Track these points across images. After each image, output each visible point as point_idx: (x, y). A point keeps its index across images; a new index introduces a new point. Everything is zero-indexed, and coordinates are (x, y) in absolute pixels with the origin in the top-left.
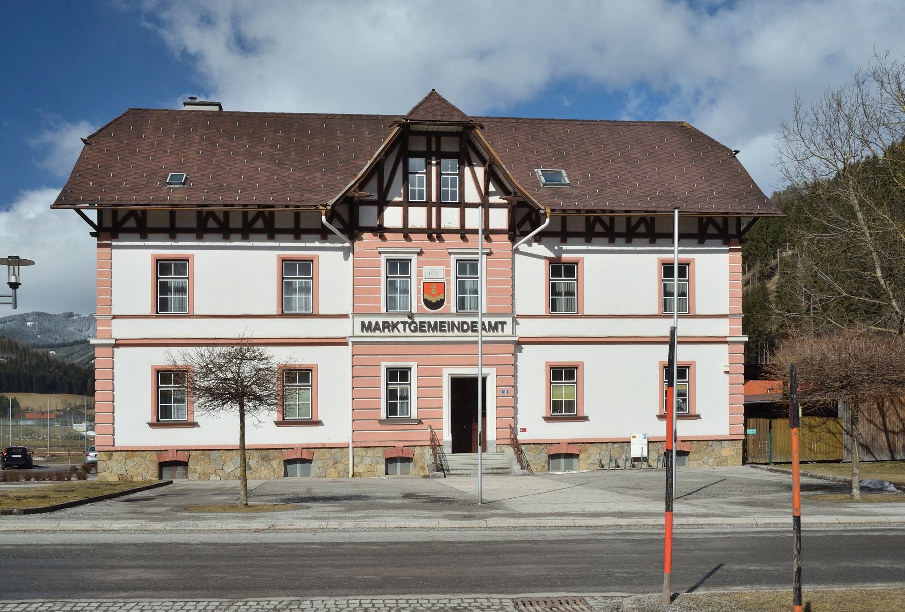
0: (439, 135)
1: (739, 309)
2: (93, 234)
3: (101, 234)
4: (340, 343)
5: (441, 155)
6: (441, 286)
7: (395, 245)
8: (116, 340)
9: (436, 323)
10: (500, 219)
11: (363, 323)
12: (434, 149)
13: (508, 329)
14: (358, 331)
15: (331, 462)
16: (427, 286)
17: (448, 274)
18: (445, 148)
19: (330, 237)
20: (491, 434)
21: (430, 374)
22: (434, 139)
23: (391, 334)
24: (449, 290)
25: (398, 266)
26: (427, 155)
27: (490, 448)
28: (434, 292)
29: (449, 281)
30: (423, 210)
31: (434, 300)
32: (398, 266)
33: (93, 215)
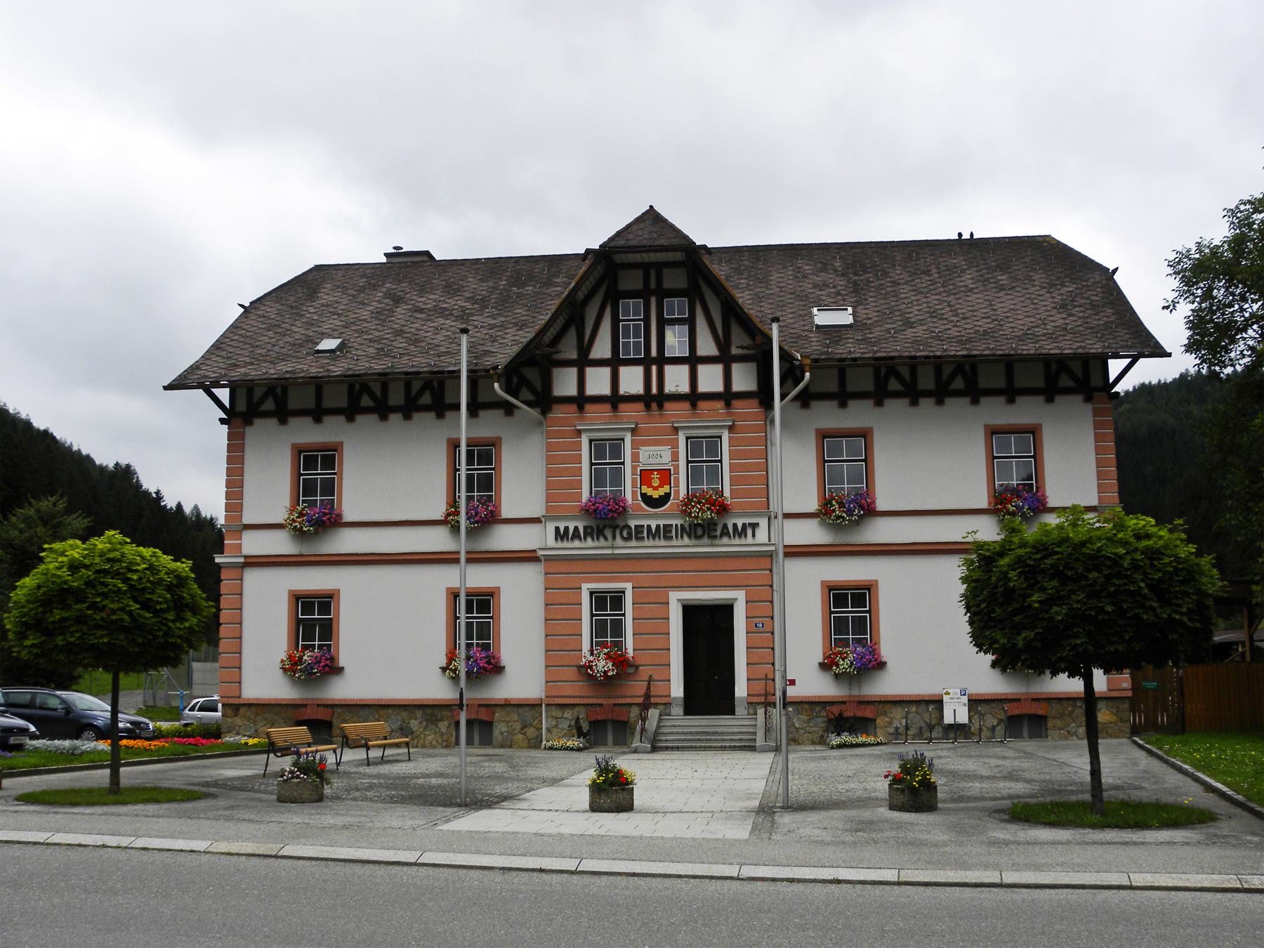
0: (659, 267)
1: (1114, 496)
2: (222, 421)
3: (234, 421)
4: (527, 557)
5: (664, 294)
6: (666, 476)
7: (598, 422)
8: (246, 557)
9: (658, 526)
10: (744, 379)
11: (557, 529)
12: (653, 285)
13: (762, 535)
14: (551, 541)
15: (518, 726)
16: (645, 476)
17: (675, 457)
18: (668, 284)
19: (515, 411)
20: (741, 689)
21: (653, 601)
22: (653, 273)
23: (596, 544)
24: (677, 480)
25: (606, 450)
26: (644, 294)
27: (740, 710)
28: (656, 483)
29: (677, 467)
30: (639, 370)
31: (656, 494)
32: (606, 450)
33: (224, 394)
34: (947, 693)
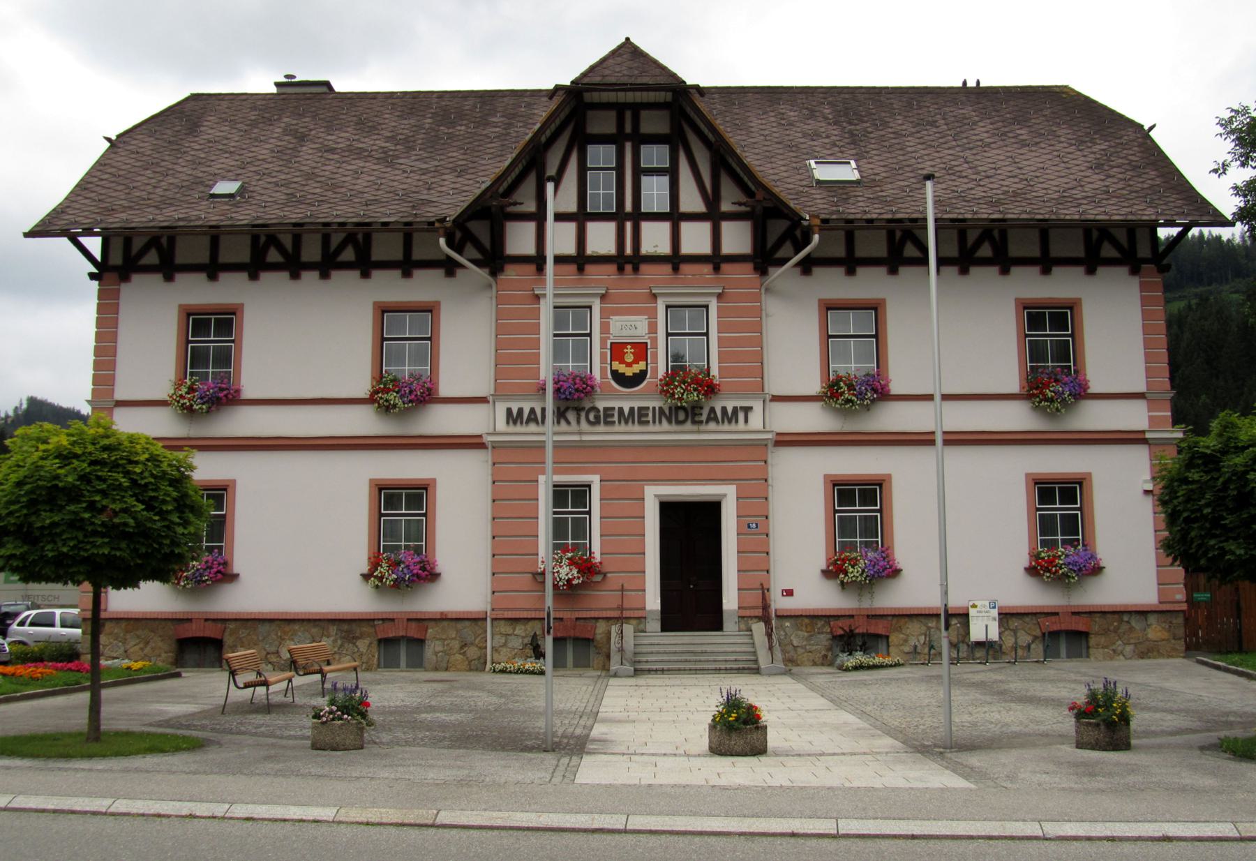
0: (637, 108)
1: (1164, 381)
2: (92, 276)
4: (471, 443)
6: (641, 351)
9: (632, 409)
10: (737, 238)
11: (509, 411)
12: (628, 129)
13: (756, 421)
14: (501, 424)
16: (617, 350)
17: (653, 328)
19: (459, 272)
20: (730, 600)
22: (628, 115)
24: (655, 355)
26: (616, 139)
27: (729, 624)
29: (655, 340)
31: (629, 372)
33: (94, 244)
34: (974, 606)
